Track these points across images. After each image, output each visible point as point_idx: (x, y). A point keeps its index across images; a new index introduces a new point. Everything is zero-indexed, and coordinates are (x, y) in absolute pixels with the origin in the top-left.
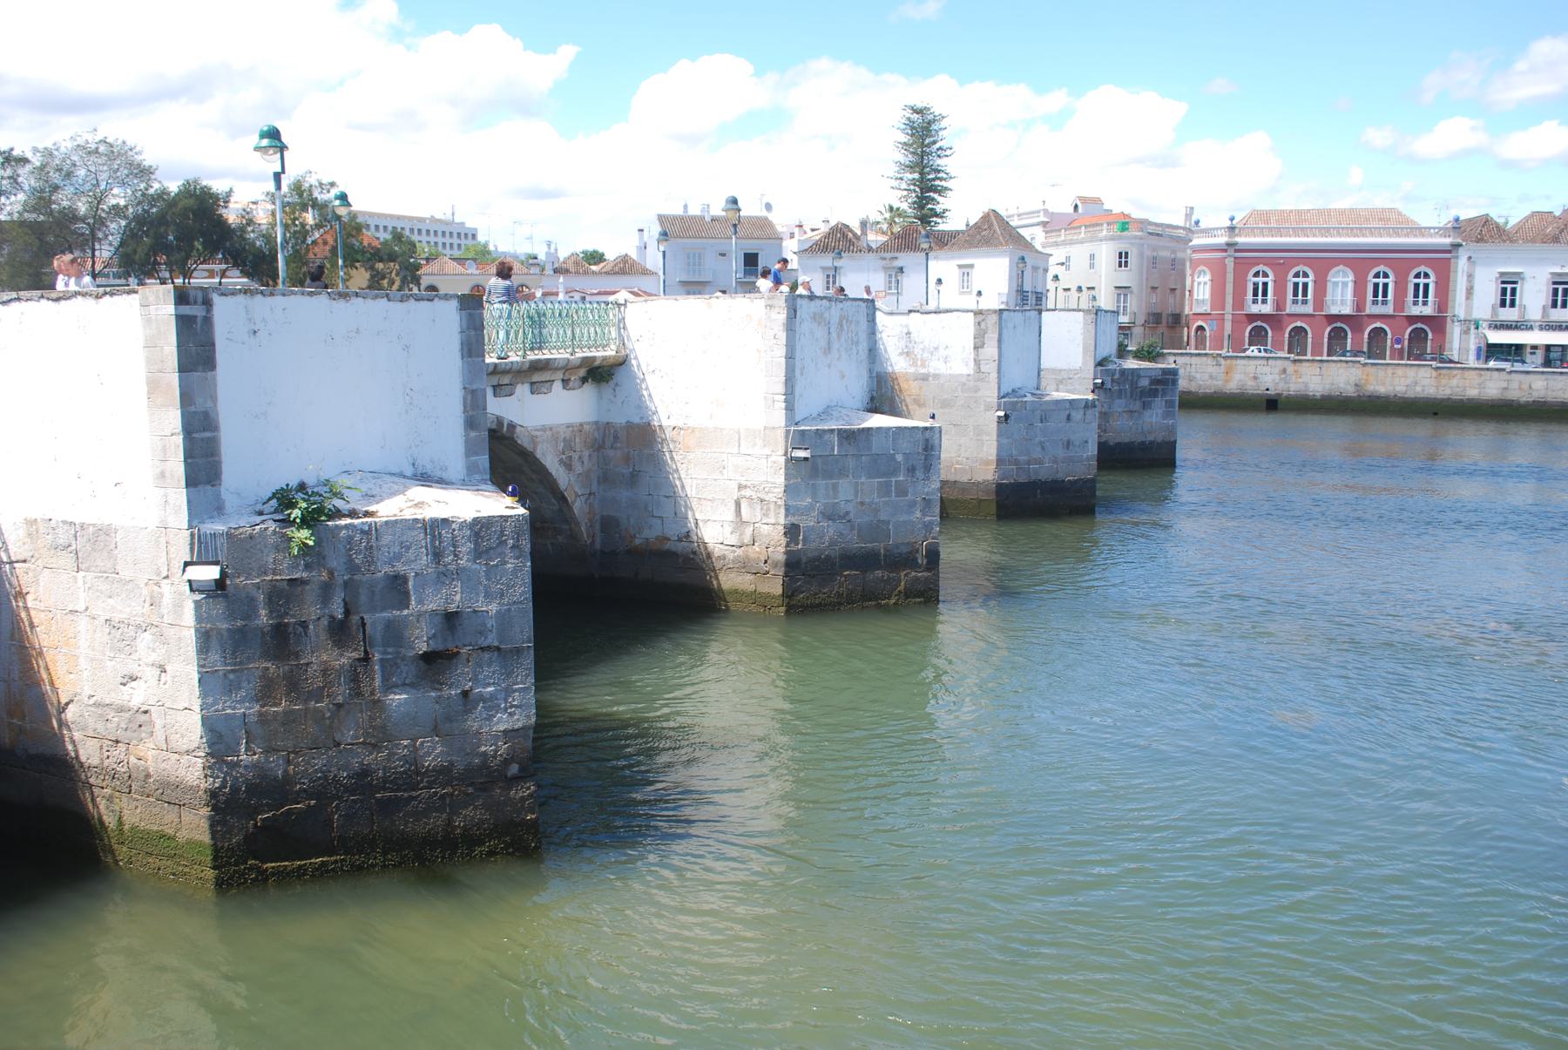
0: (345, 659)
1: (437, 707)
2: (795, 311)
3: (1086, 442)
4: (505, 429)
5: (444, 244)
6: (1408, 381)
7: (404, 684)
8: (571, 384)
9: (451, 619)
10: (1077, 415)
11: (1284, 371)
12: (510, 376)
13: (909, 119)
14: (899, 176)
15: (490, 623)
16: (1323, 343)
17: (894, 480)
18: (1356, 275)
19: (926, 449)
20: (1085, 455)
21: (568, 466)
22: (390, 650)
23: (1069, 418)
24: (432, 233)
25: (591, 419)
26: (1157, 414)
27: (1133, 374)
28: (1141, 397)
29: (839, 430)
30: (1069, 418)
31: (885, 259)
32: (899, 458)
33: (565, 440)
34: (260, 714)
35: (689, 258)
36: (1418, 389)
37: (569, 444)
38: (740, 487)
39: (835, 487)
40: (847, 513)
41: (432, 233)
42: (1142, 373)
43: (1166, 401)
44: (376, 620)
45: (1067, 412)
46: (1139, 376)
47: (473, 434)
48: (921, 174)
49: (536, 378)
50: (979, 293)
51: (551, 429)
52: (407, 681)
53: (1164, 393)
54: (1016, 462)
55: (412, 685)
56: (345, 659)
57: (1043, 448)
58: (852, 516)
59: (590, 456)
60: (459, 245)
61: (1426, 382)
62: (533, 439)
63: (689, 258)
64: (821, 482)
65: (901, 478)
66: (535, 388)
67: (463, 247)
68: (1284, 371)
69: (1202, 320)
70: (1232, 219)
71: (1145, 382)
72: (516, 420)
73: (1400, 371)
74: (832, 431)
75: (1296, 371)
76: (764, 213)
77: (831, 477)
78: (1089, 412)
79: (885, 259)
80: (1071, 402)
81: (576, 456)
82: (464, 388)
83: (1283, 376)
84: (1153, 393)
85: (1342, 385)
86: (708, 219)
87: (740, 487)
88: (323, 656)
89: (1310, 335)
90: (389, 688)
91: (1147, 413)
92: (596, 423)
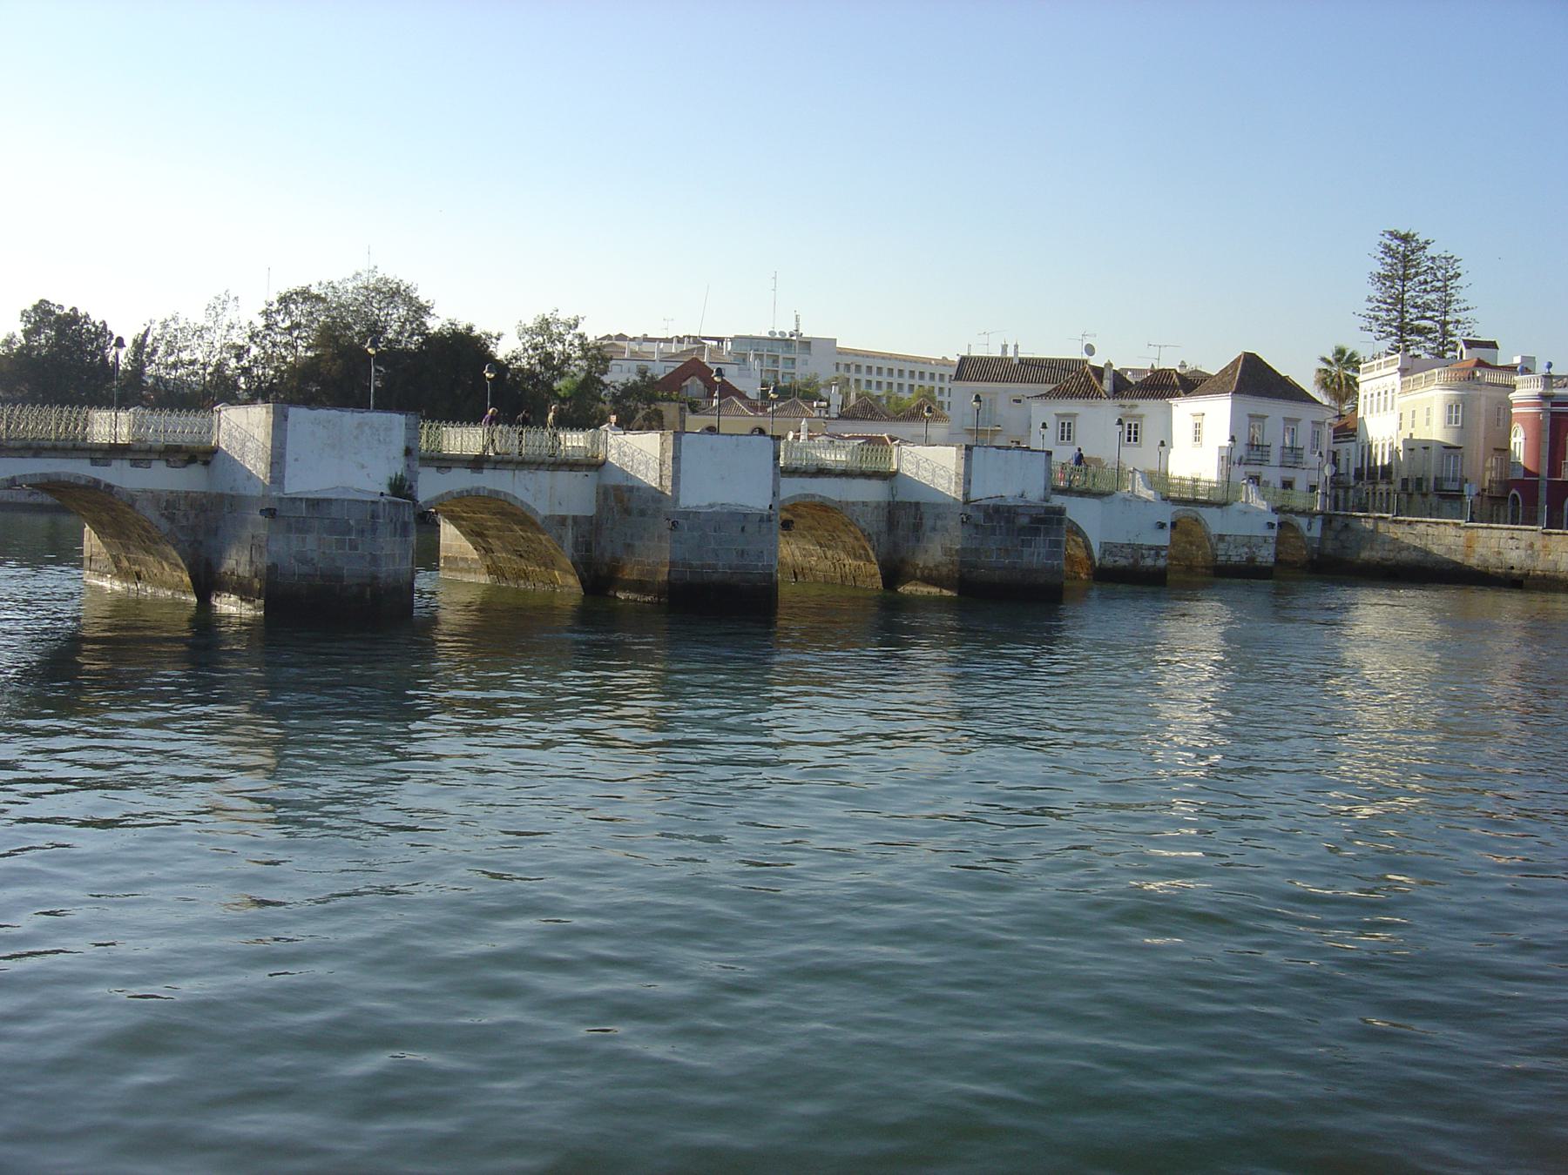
5: (879, 384)
11: (1531, 546)
13: (1387, 247)
14: (1372, 314)
20: (760, 564)
21: (171, 519)
24: (937, 377)
25: (203, 489)
26: (1039, 555)
28: (1019, 535)
29: (307, 499)
31: (1123, 406)
32: (352, 522)
33: (167, 501)
38: (253, 537)
39: (304, 540)
40: (312, 559)
41: (937, 377)
42: (1020, 510)
46: (1017, 514)
48: (1402, 312)
54: (690, 566)
58: (315, 561)
60: (911, 386)
67: (916, 387)
68: (1531, 546)
71: (1024, 521)
72: (113, 482)
74: (301, 499)
76: (1085, 357)
78: (764, 525)
79: (1123, 406)
83: (1529, 552)
84: (1035, 532)
86: (1016, 362)
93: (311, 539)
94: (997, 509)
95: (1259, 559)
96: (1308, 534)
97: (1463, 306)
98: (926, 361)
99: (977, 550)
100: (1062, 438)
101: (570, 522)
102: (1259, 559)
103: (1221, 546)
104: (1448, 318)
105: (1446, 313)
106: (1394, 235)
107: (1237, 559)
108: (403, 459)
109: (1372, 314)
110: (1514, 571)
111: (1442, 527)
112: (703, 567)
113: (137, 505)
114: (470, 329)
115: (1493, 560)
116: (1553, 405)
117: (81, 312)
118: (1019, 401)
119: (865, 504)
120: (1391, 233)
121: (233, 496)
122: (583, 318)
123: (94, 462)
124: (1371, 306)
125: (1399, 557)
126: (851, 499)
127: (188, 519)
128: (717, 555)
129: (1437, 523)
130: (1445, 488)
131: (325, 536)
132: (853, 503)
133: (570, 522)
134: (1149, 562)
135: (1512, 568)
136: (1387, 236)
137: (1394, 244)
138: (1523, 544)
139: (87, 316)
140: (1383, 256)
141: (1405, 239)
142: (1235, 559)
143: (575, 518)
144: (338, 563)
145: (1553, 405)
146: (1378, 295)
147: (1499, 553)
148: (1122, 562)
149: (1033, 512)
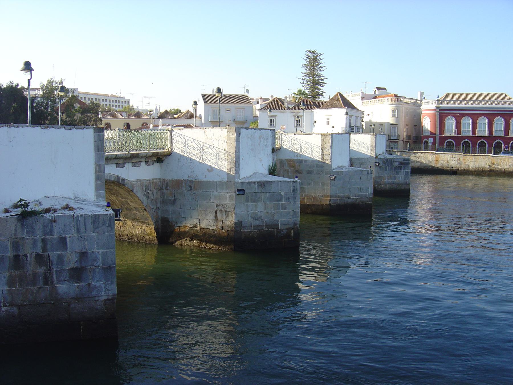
0: (41, 270)
1: (78, 289)
2: (240, 134)
3: (368, 188)
4: (121, 181)
5: (116, 106)
7: (65, 280)
8: (149, 163)
9: (83, 255)
10: (364, 177)
11: (459, 159)
12: (123, 160)
13: (309, 56)
14: (304, 78)
15: (99, 257)
17: (280, 203)
18: (456, 120)
19: (294, 190)
21: (147, 196)
22: (60, 267)
23: (360, 178)
24: (111, 101)
25: (158, 177)
27: (391, 161)
28: (395, 170)
29: (258, 182)
30: (360, 178)
31: (294, 112)
32: (283, 194)
34: (9, 290)
35: (214, 112)
37: (147, 188)
38: (217, 206)
39: (256, 206)
40: (261, 216)
41: (111, 101)
42: (395, 160)
43: (405, 171)
44: (54, 255)
45: (360, 176)
47: (99, 182)
49: (134, 161)
50: (333, 127)
51: (140, 181)
52: (66, 279)
53: (404, 169)
54: (339, 197)
55: (68, 281)
56: (41, 270)
57: (350, 191)
58: (263, 218)
59: (157, 192)
60: (122, 106)
62: (132, 185)
63: (214, 112)
64: (250, 204)
65: (284, 202)
66: (134, 165)
67: (124, 106)
68: (459, 159)
70: (438, 97)
71: (396, 164)
72: (126, 177)
73: (506, 160)
74: (254, 182)
75: (464, 160)
76: (246, 94)
77: (254, 202)
78: (369, 176)
79: (294, 112)
80: (361, 171)
81: (150, 192)
82: (96, 164)
83: (459, 162)
84: (400, 168)
85: (483, 165)
87: (217, 206)
88: (31, 267)
90: (60, 281)
91: (398, 176)
92: (160, 179)
93: (260, 206)
98: (107, 96)
99: (380, 177)
100: (271, 125)
106: (310, 52)
108: (271, 155)
110: (453, 168)
111: (427, 154)
112: (344, 196)
113: (135, 191)
114: (18, 85)
115: (446, 165)
116: (440, 110)
118: (229, 111)
120: (309, 51)
121: (191, 181)
122: (65, 80)
123: (118, 165)
127: (154, 195)
128: (350, 191)
129: (425, 153)
130: (391, 139)
131: (268, 203)
135: (453, 167)
136: (307, 52)
137: (310, 54)
138: (456, 159)
140: (306, 58)
141: (313, 53)
144: (276, 218)
145: (440, 110)
146: (305, 71)
147: (448, 162)
149: (400, 160)
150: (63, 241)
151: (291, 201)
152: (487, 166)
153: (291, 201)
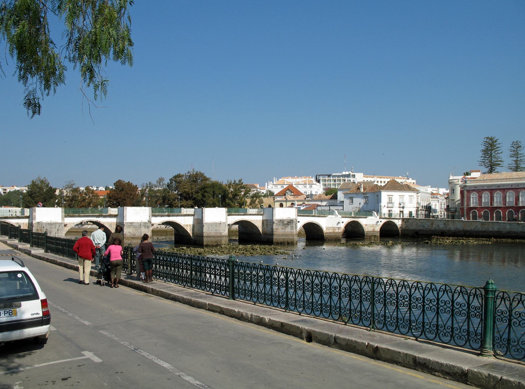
6: (475, 226)
11: (445, 224)
16: (489, 216)
36: (477, 229)
44: (42, 229)
54: (207, 233)
61: (479, 226)
68: (445, 224)
69: (512, 209)
71: (286, 222)
81: (112, 226)
84: (288, 224)
89: (502, 213)
93: (131, 229)
94: (280, 220)
95: (376, 230)
96: (398, 224)
97: (523, 155)
101: (189, 225)
102: (376, 230)
103: (366, 227)
104: (518, 159)
105: (517, 158)
106: (487, 138)
107: (370, 230)
109: (482, 161)
115: (437, 228)
117: (131, 182)
119: (257, 220)
124: (482, 158)
125: (418, 228)
126: (253, 219)
132: (254, 220)
133: (189, 225)
134: (337, 231)
138: (443, 224)
139: (132, 183)
141: (491, 139)
142: (370, 230)
143: (190, 225)
148: (331, 231)
150: (44, 227)
151: (140, 228)
152: (461, 228)
153: (140, 228)
